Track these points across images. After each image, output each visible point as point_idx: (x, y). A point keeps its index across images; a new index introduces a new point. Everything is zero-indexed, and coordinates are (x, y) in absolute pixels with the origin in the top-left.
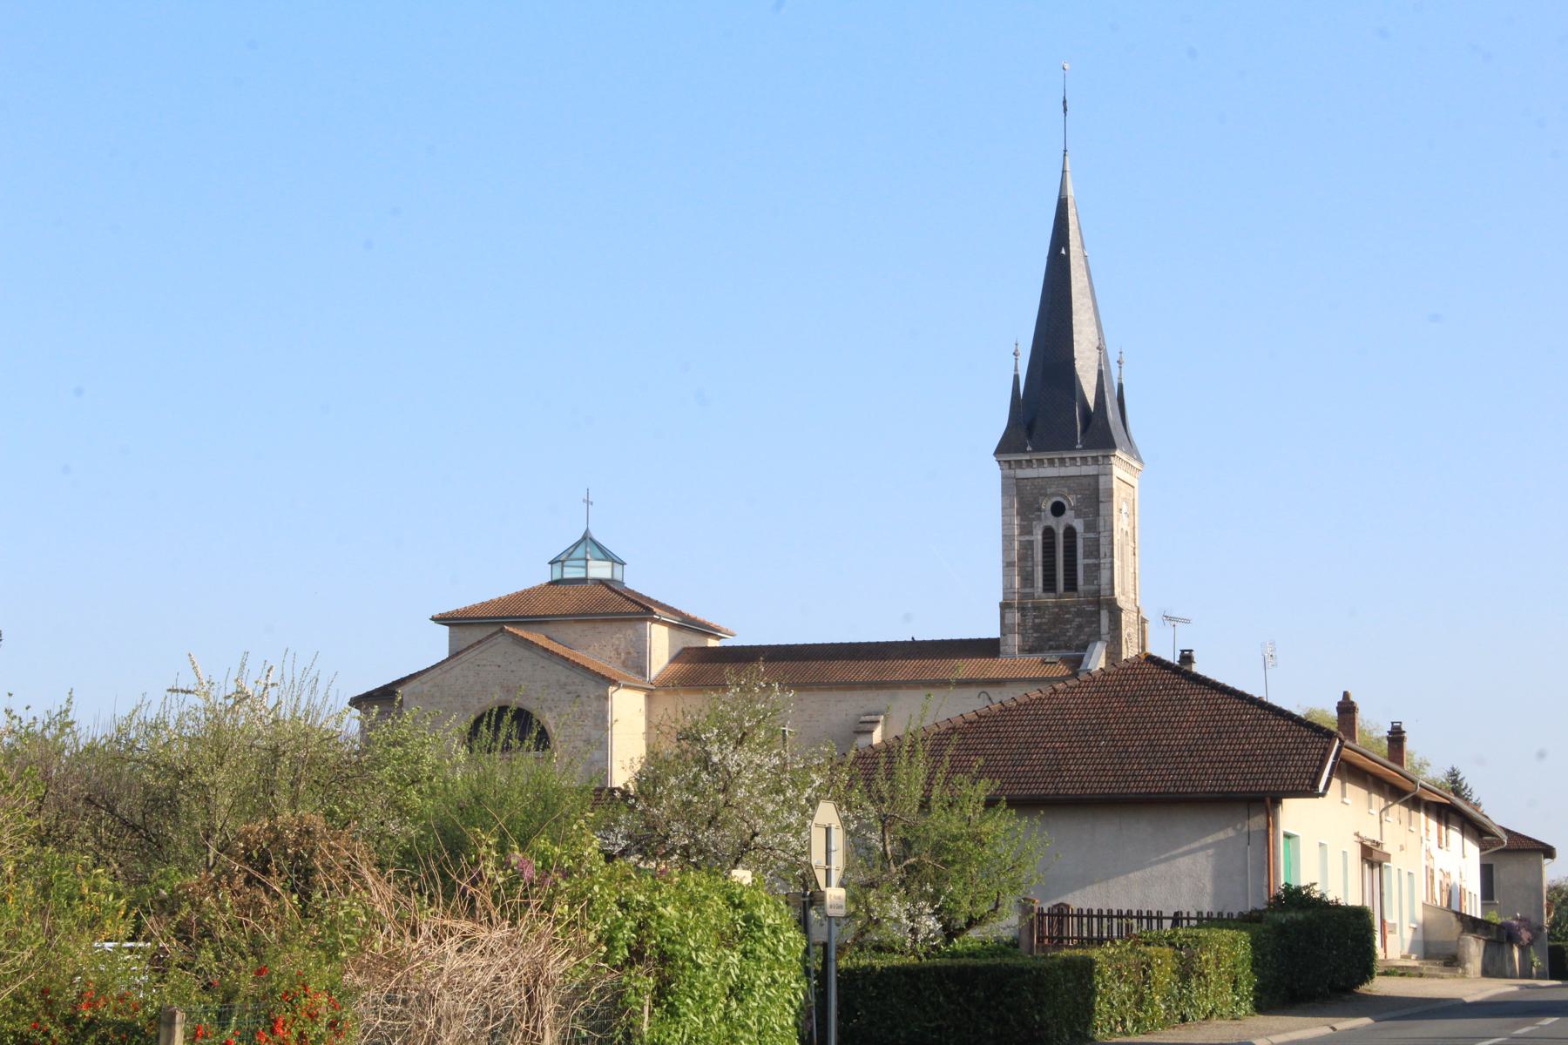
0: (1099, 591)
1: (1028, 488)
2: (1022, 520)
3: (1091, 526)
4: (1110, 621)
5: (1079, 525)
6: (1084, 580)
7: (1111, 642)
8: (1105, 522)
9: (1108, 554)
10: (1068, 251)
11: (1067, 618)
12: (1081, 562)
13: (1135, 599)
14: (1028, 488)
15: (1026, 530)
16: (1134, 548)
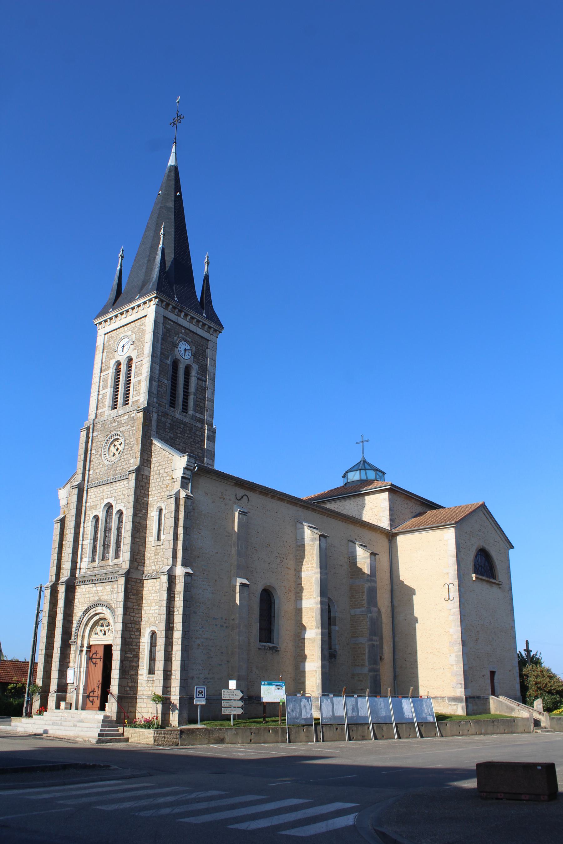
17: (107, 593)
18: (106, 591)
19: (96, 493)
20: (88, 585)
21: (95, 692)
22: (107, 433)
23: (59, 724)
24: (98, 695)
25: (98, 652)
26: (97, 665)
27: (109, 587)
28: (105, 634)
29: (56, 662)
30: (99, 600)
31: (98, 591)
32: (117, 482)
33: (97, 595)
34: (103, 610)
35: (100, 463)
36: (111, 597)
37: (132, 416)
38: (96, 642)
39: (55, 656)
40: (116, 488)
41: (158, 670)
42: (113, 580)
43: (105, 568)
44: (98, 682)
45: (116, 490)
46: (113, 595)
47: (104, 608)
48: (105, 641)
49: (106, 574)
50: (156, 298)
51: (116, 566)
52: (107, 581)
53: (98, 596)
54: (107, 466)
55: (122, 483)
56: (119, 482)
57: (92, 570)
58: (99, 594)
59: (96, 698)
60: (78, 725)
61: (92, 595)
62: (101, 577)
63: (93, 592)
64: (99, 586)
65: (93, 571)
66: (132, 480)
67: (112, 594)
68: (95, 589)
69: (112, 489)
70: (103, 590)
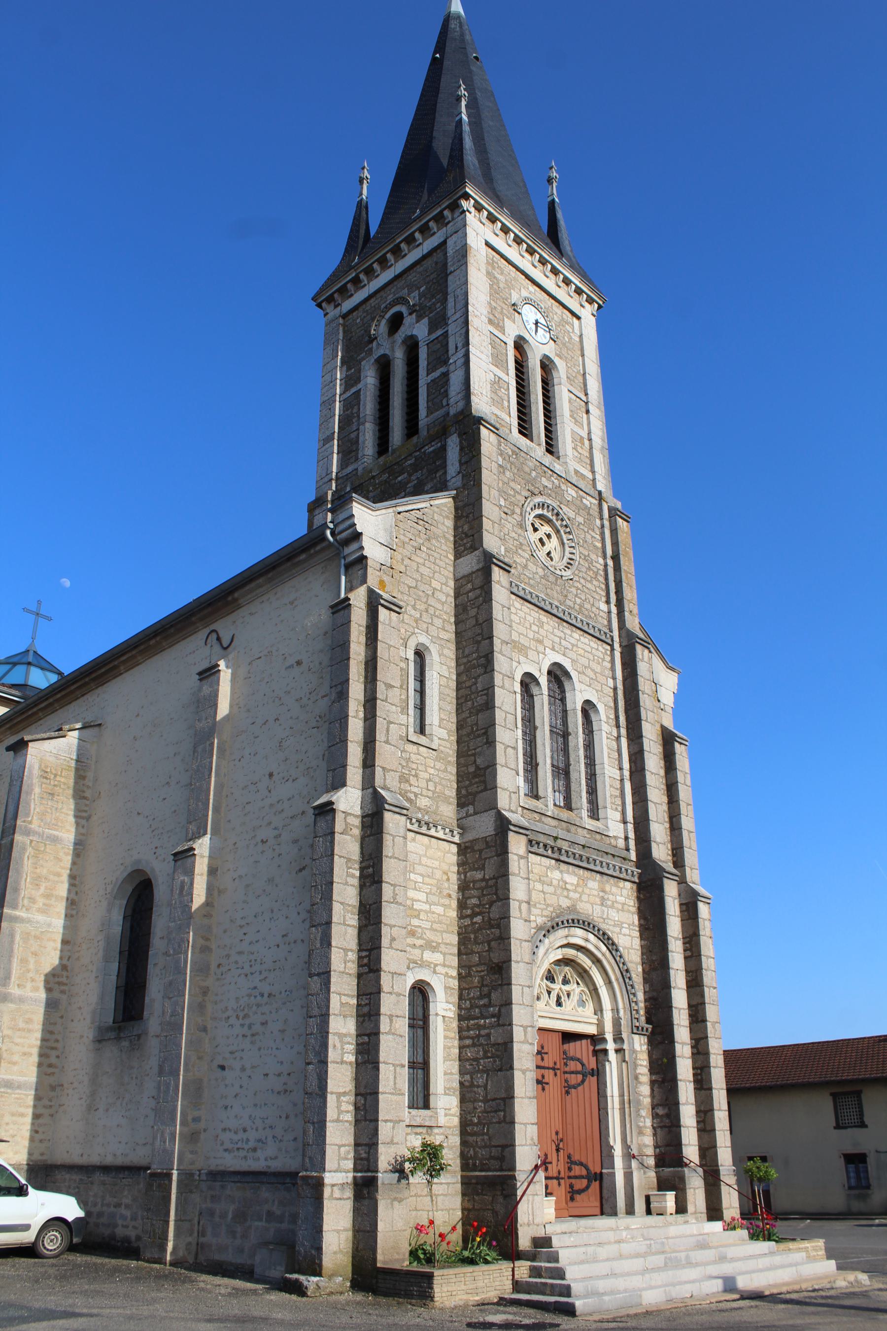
0: (448, 413)
1: (358, 321)
2: (349, 369)
3: (439, 321)
4: (462, 449)
5: (420, 330)
6: (428, 407)
7: (464, 486)
8: (455, 297)
9: (460, 345)
10: (442, 56)
11: (400, 482)
12: (424, 379)
13: (594, 480)
14: (358, 321)
15: (351, 381)
16: (587, 403)
17: (592, 899)
18: (587, 891)
19: (522, 614)
20: (539, 857)
21: (551, 1163)
22: (532, 488)
23: (684, 1262)
24: (559, 1172)
25: (545, 1050)
26: (546, 1086)
27: (594, 883)
28: (559, 1004)
29: (524, 1072)
30: (572, 909)
31: (566, 883)
32: (574, 629)
33: (565, 893)
34: (587, 940)
35: (521, 544)
36: (603, 912)
37: (584, 501)
38: (548, 1020)
39: (519, 1050)
40: (573, 641)
41: (719, 1110)
42: (605, 870)
43: (573, 828)
44: (554, 1137)
45: (573, 645)
46: (605, 909)
47: (591, 937)
48: (571, 1024)
49: (584, 846)
50: (600, 307)
51: (598, 837)
52: (591, 866)
53: (567, 897)
54: (544, 570)
55: (586, 641)
56: (578, 631)
57: (536, 816)
58: (572, 894)
59: (555, 1182)
60: (729, 1256)
61: (551, 889)
62: (569, 847)
63: (555, 882)
64: (568, 873)
65: (540, 821)
66: (642, 660)
67: (602, 904)
68: (556, 875)
69: (562, 635)
70: (578, 885)
